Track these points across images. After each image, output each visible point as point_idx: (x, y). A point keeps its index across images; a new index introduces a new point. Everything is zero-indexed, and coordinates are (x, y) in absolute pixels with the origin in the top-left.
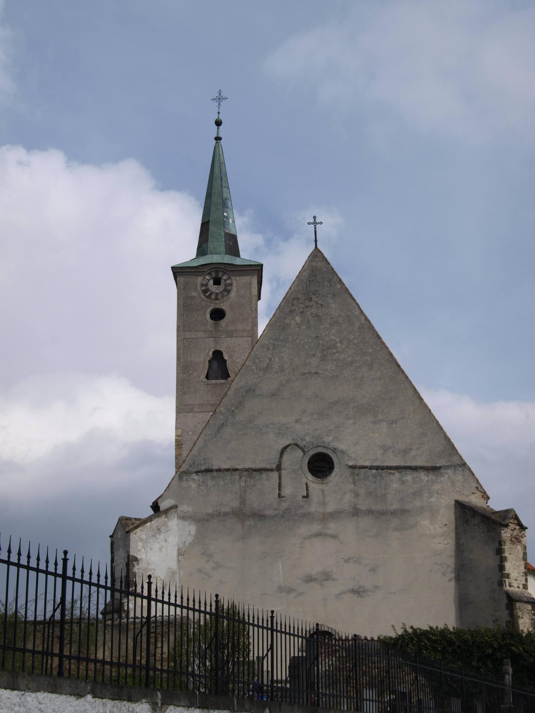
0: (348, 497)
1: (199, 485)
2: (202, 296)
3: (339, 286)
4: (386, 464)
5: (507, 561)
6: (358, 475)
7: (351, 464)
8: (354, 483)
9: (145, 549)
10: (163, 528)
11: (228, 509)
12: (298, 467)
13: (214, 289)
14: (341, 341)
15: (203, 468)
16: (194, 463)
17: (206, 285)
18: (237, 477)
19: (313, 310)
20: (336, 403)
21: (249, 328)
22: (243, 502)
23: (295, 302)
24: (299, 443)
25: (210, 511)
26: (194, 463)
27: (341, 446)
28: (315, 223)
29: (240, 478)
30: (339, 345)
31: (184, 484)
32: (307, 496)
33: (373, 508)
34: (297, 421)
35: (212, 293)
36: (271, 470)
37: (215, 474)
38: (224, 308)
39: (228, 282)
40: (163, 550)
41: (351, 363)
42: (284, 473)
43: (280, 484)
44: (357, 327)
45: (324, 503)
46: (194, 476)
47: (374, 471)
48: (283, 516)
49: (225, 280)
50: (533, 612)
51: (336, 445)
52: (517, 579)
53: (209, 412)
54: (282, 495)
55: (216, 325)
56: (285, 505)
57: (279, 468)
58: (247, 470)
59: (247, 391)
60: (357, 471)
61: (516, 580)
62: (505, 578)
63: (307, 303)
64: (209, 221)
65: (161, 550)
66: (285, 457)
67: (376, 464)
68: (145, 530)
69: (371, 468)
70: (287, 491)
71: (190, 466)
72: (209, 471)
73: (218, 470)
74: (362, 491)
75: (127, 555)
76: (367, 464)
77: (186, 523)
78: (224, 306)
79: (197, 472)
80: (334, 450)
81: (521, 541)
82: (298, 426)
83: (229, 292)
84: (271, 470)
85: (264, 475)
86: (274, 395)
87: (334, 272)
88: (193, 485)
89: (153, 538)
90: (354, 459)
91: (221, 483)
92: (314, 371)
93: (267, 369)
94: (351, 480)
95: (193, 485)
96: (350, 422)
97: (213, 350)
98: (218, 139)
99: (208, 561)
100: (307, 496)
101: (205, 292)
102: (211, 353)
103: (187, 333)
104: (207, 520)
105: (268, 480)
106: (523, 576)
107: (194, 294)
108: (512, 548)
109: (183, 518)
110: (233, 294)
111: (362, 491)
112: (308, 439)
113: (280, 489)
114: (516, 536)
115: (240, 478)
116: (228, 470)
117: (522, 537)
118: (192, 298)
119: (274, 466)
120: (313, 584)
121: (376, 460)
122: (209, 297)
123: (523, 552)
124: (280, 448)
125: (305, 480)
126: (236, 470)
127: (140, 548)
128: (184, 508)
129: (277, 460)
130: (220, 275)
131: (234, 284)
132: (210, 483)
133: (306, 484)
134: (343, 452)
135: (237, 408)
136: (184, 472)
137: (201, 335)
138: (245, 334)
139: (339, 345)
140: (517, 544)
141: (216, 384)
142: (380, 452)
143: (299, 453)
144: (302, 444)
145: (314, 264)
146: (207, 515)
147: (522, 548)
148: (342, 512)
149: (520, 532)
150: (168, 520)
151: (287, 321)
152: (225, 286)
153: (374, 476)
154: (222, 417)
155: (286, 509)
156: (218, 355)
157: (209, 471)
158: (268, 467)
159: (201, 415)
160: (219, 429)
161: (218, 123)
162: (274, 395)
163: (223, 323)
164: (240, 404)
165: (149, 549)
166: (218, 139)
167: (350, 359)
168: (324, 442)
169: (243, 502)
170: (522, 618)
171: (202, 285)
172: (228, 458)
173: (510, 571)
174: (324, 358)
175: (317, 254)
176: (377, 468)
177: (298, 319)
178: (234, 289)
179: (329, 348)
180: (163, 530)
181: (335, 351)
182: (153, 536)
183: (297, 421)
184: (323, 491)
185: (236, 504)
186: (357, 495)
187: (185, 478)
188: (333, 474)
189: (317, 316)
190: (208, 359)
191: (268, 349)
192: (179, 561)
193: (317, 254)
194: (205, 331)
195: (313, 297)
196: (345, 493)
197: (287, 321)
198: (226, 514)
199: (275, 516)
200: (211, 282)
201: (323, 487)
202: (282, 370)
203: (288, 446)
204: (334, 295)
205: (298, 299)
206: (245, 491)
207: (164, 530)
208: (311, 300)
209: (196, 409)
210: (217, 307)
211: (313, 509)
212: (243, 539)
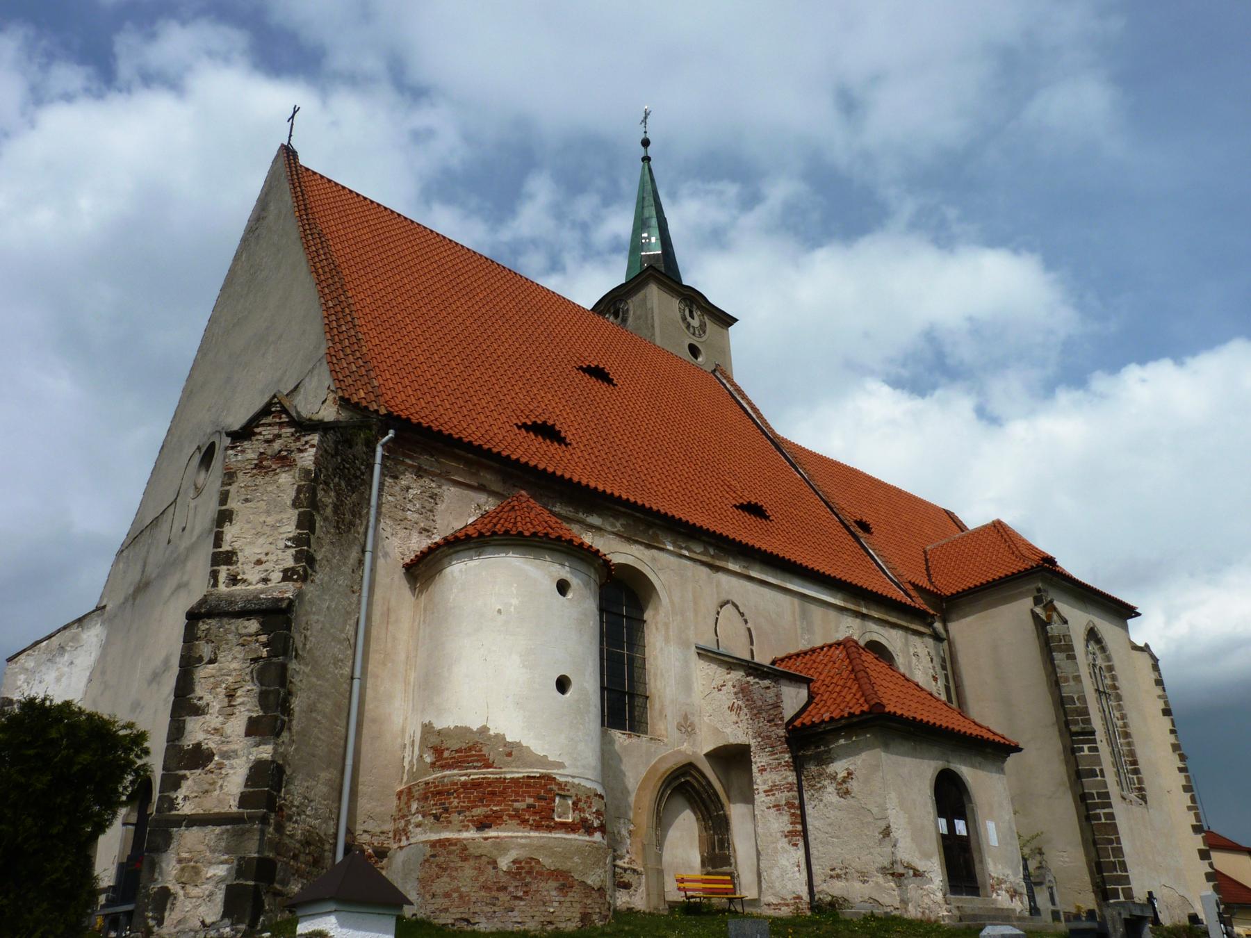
5: (231, 521)
9: (28, 683)
10: (71, 644)
40: (63, 679)
50: (263, 638)
52: (264, 558)
61: (259, 562)
62: (219, 565)
65: (58, 680)
68: (36, 653)
81: (294, 460)
89: (49, 664)
106: (287, 547)
108: (256, 485)
110: (630, 320)
114: (280, 451)
117: (300, 451)
123: (296, 486)
127: (19, 683)
140: (278, 471)
147: (294, 477)
149: (298, 439)
150: (83, 630)
165: (37, 682)
170: (212, 661)
173: (236, 545)
180: (68, 649)
182: (49, 660)
207: (72, 647)
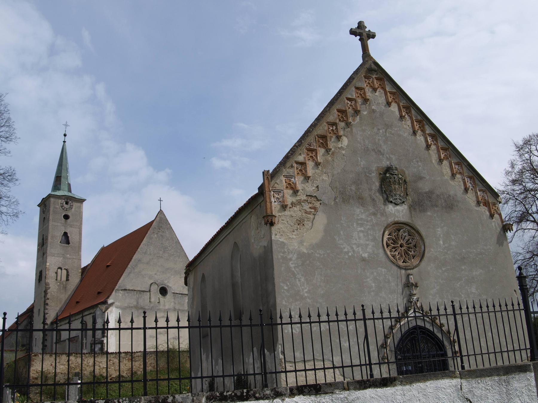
0: (172, 304)
1: (122, 295)
2: (61, 208)
3: (169, 226)
4: (184, 293)
6: (175, 296)
7: (173, 292)
8: (174, 299)
11: (132, 305)
12: (156, 291)
13: (66, 206)
14: (169, 246)
15: (123, 288)
16: (120, 286)
17: (63, 204)
18: (136, 293)
19: (161, 233)
20: (168, 269)
21: (79, 225)
22: (138, 303)
23: (155, 229)
24: (156, 282)
25: (126, 305)
26: (120, 286)
27: (170, 285)
28: (160, 200)
29: (137, 294)
30: (169, 248)
31: (117, 294)
32: (159, 302)
33: (180, 308)
34: (155, 274)
35: (65, 208)
36: (147, 292)
37: (128, 291)
38: (69, 215)
39: (72, 204)
41: (173, 255)
42: (151, 293)
43: (150, 297)
44: (175, 242)
45: (164, 306)
46: (121, 291)
47: (180, 295)
48: (151, 309)
49: (70, 203)
51: (168, 284)
53: (61, 257)
54: (151, 301)
55: (66, 221)
56: (152, 305)
57: (150, 291)
58: (139, 291)
59: (139, 261)
60: (175, 295)
63: (159, 230)
64: (61, 176)
66: (152, 287)
67: (181, 293)
69: (179, 294)
70: (153, 300)
71: (119, 287)
72: (125, 290)
73: (129, 290)
74: (177, 302)
75: (103, 321)
76: (178, 292)
77: (118, 310)
78: (69, 214)
79: (122, 290)
80: (168, 286)
82: (156, 276)
83: (72, 208)
84: (147, 292)
85: (145, 293)
86: (147, 263)
87: (167, 220)
88: (120, 295)
90: (174, 290)
91: (130, 295)
92: (161, 256)
93: (145, 253)
94: (173, 297)
95: (120, 295)
96: (173, 276)
97: (64, 232)
98: (64, 142)
99: (126, 325)
100: (159, 302)
101: (62, 207)
102: (63, 233)
103: (54, 223)
104: (125, 309)
105: (146, 295)
107: (58, 207)
109: (117, 307)
110: (73, 210)
111: (177, 302)
112: (159, 281)
113: (150, 299)
115: (137, 294)
116: (132, 290)
118: (56, 208)
119: (148, 290)
120: (161, 335)
121: (180, 291)
122: (63, 209)
124: (150, 283)
125: (158, 296)
126: (135, 290)
128: (117, 304)
129: (149, 288)
130: (69, 201)
131: (74, 206)
132: (126, 294)
133: (159, 298)
134: (170, 287)
135: (135, 267)
136: (117, 289)
137: (59, 224)
138: (77, 227)
139: (169, 248)
141: (64, 246)
142: (182, 288)
143: (157, 286)
144: (157, 283)
145: (161, 216)
146: (125, 307)
148: (170, 309)
151: (152, 236)
152: (70, 205)
153: (181, 297)
154: (130, 269)
155: (152, 307)
156: (65, 234)
157: (125, 290)
158: (146, 290)
159: (57, 258)
160: (129, 274)
161: (65, 135)
162: (147, 263)
163: (69, 221)
164: (136, 265)
166: (64, 142)
167: (172, 253)
168: (164, 283)
169: (138, 303)
171: (61, 204)
172: (132, 286)
174: (164, 252)
175: (161, 212)
176: (181, 294)
177: (156, 235)
178: (74, 207)
179: (166, 248)
181: (168, 249)
183: (155, 274)
184: (164, 301)
185: (135, 303)
186: (175, 303)
187: (117, 292)
188: (168, 295)
189: (162, 236)
190: (62, 235)
191: (146, 245)
192: (115, 324)
193: (161, 212)
194: (61, 223)
195: (161, 228)
196: (171, 302)
197: (152, 236)
198: (132, 307)
199: (149, 309)
200: (65, 203)
201: (164, 299)
202: (151, 254)
203: (153, 283)
204: (167, 229)
205: (156, 228)
206: (138, 299)
208: (160, 229)
209: (56, 255)
210: (66, 214)
211: (161, 307)
212: (138, 317)
